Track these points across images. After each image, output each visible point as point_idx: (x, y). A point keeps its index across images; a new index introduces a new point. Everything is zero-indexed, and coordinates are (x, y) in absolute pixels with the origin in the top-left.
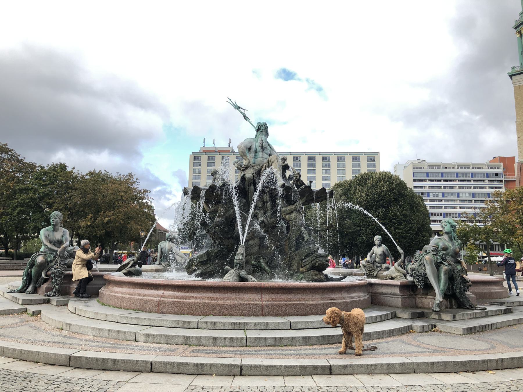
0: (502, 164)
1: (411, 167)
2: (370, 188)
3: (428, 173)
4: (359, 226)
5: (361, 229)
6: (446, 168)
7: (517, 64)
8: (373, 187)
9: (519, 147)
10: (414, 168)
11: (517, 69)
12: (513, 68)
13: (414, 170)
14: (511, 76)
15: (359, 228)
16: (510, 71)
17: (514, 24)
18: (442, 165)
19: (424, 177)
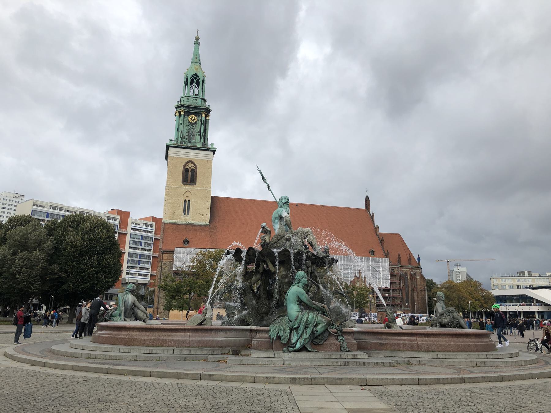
0: (119, 217)
1: (31, 203)
2: (87, 232)
3: (48, 214)
4: (66, 272)
5: (68, 276)
6: (68, 211)
7: (174, 139)
8: (91, 231)
9: (164, 209)
10: (34, 205)
11: (173, 142)
12: (171, 140)
13: (34, 207)
14: (168, 147)
15: (65, 275)
16: (168, 142)
17: (176, 104)
18: (64, 208)
19: (43, 217)
